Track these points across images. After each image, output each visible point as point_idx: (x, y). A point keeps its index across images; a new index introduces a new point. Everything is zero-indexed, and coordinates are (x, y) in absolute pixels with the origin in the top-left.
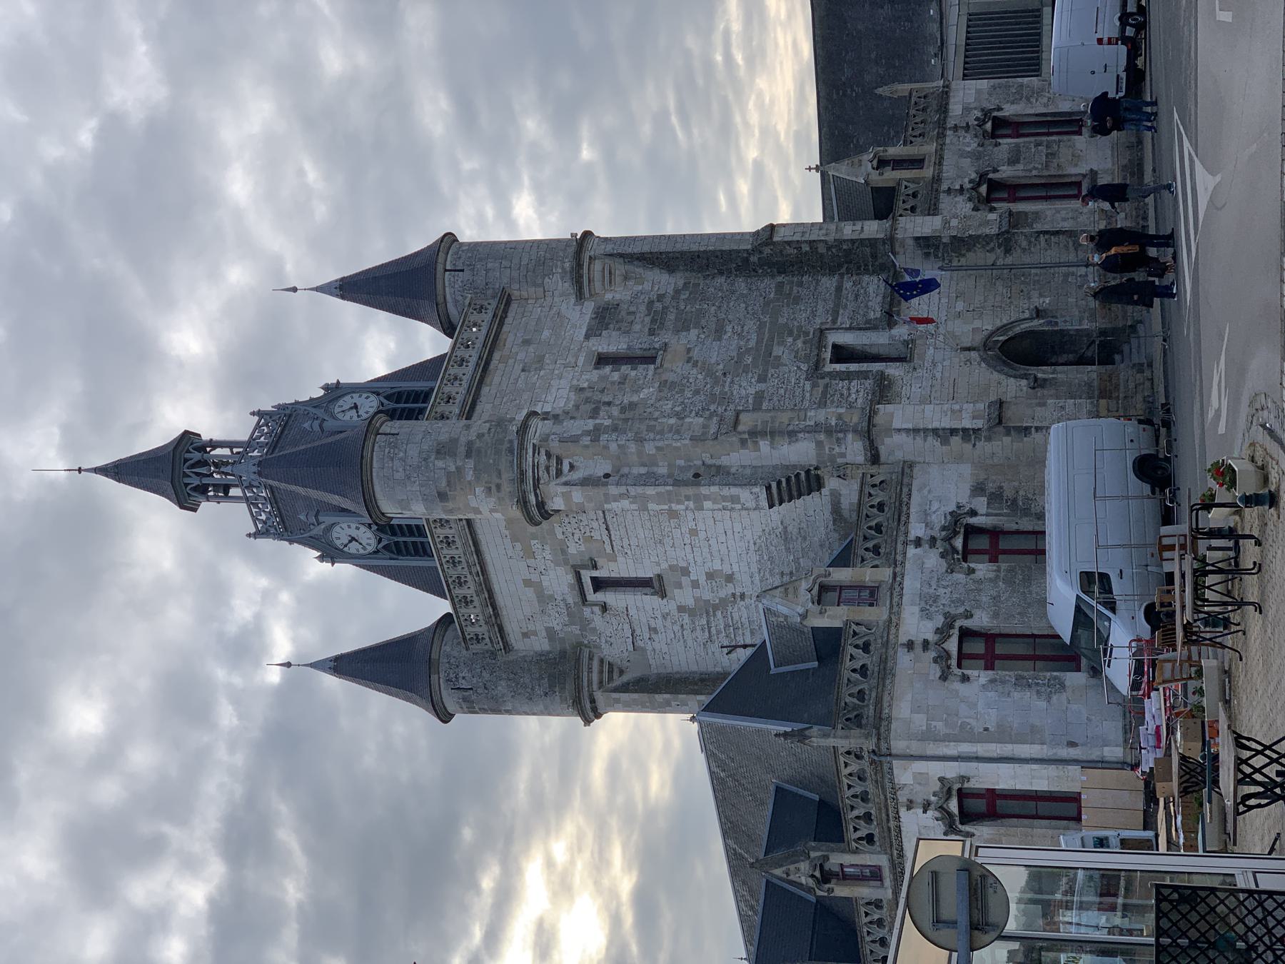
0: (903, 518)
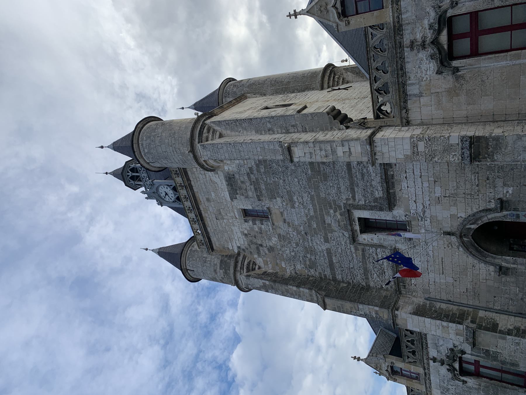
0: (424, 346)
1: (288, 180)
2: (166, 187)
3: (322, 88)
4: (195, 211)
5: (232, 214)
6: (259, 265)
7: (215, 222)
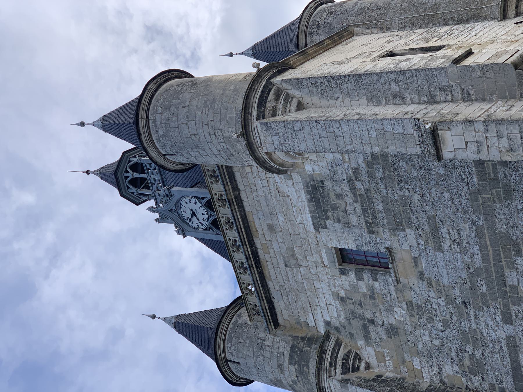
1: (430, 194)
2: (193, 200)
3: (504, 17)
4: (246, 249)
5: (317, 257)
6: (368, 361)
7: (282, 271)
